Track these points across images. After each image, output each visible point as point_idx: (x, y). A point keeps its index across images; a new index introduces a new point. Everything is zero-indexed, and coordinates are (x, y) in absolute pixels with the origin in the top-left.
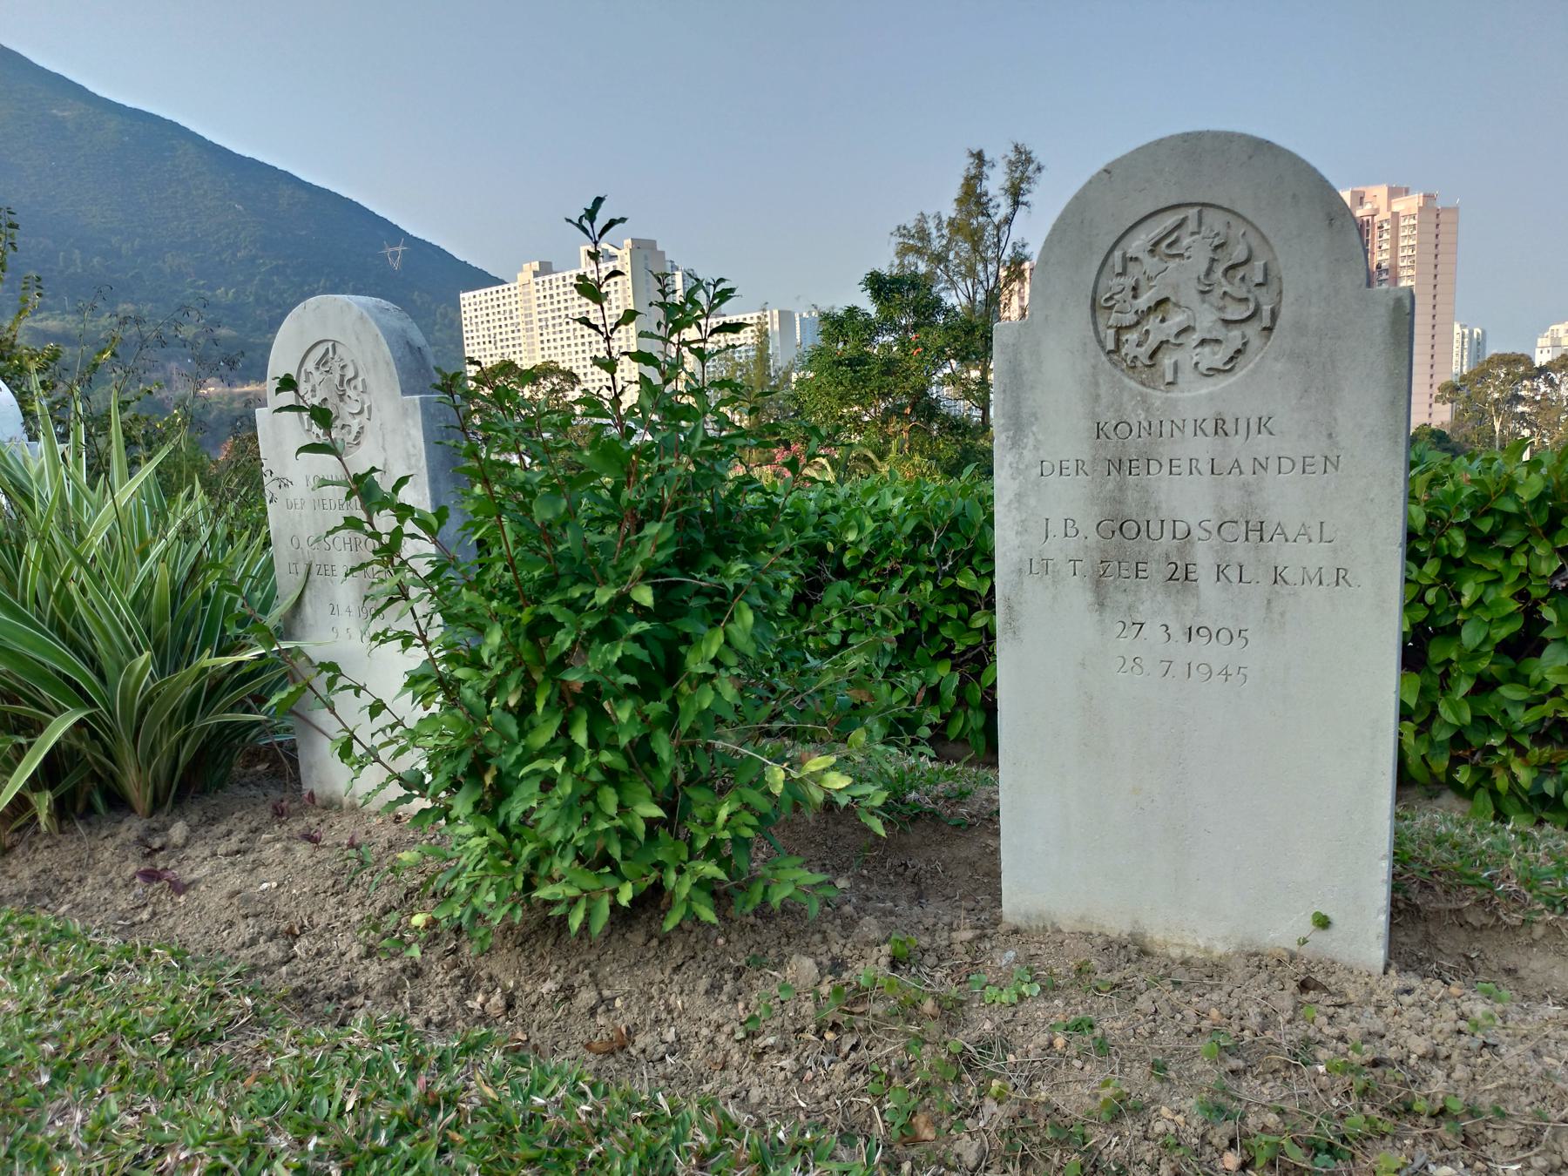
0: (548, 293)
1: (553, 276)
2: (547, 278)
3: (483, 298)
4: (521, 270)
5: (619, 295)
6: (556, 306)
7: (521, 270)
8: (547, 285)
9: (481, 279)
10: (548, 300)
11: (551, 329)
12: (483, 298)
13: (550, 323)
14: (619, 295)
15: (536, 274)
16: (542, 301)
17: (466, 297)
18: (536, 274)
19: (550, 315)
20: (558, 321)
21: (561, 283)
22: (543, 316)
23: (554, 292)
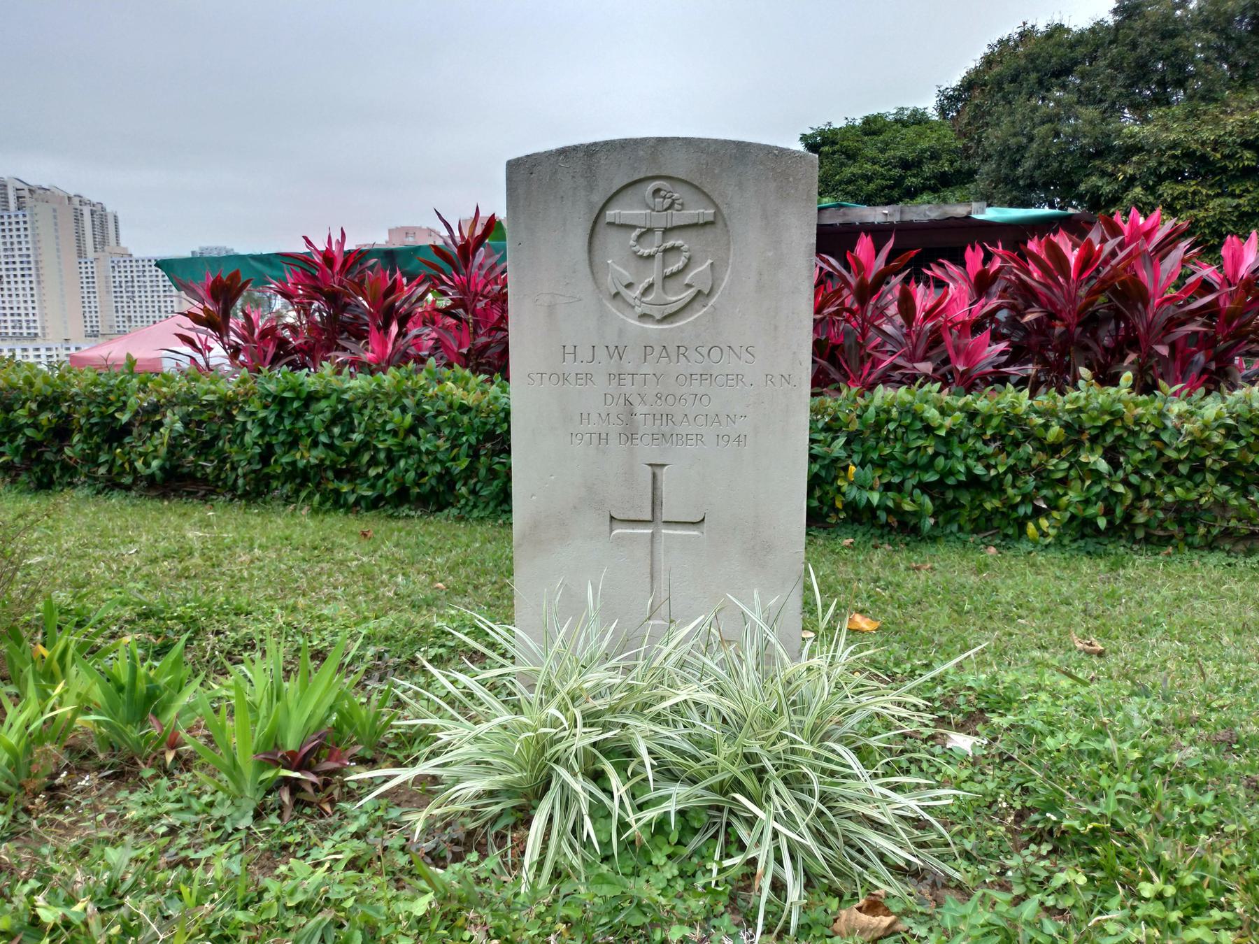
14: (29, 239)
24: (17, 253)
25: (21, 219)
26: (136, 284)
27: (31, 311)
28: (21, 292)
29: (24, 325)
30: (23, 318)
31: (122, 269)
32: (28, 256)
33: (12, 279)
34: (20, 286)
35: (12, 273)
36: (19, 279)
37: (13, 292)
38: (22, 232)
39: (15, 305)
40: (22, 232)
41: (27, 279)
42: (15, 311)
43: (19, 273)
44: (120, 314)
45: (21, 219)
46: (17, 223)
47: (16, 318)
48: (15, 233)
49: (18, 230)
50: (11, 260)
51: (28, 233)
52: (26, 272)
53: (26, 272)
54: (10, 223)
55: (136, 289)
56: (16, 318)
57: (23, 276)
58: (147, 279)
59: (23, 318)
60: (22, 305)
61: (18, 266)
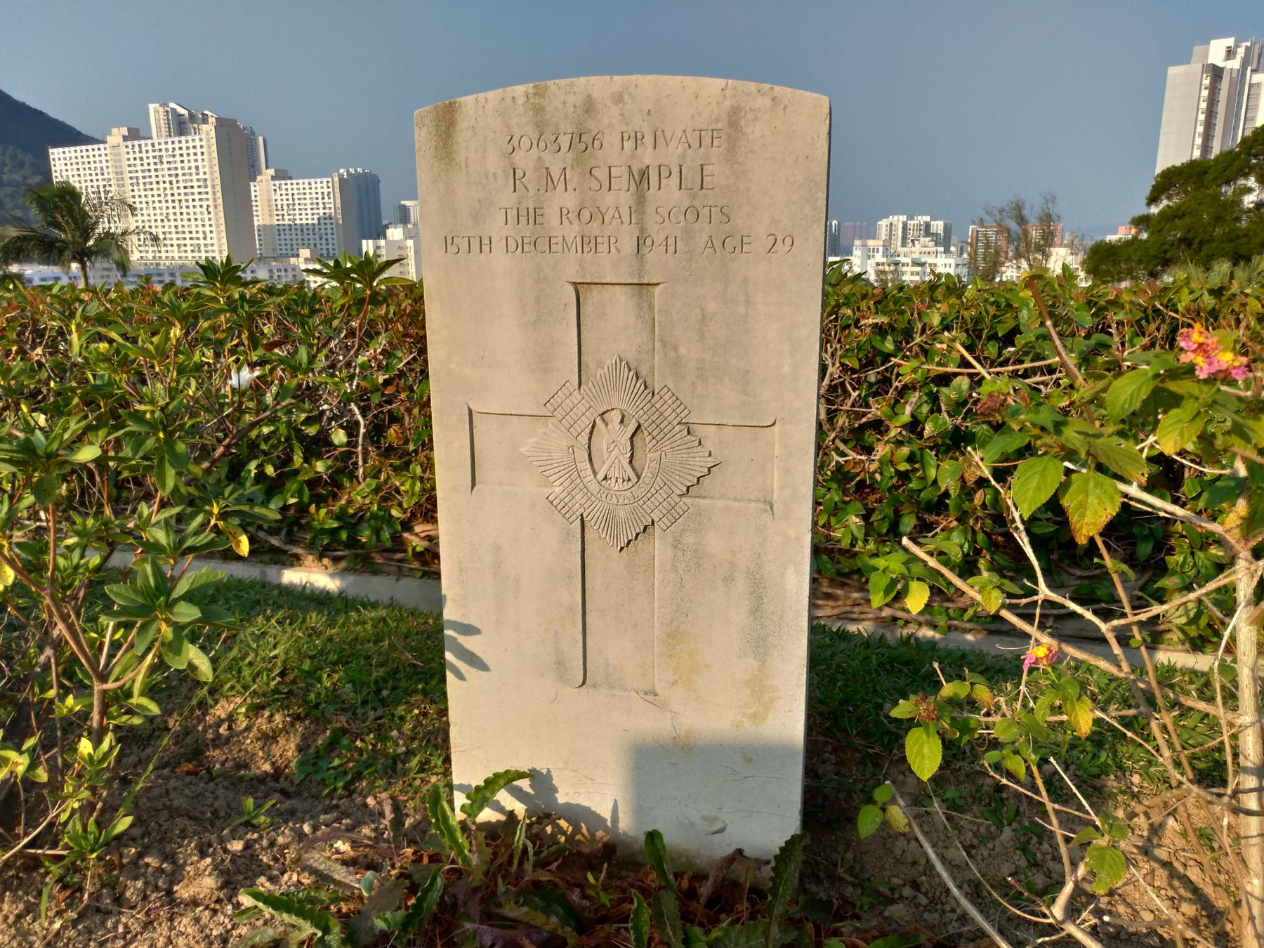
0: (138, 155)
1: (142, 142)
2: (136, 143)
3: (73, 155)
4: (110, 134)
5: (206, 163)
6: (146, 167)
7: (110, 134)
8: (137, 149)
9: (71, 137)
10: (138, 162)
11: (142, 187)
12: (73, 155)
13: (141, 181)
14: (206, 163)
15: (125, 139)
16: (132, 162)
17: (55, 154)
18: (125, 139)
19: (140, 174)
20: (148, 180)
21: (150, 148)
22: (134, 175)
23: (144, 155)
24: (194, 177)
25: (198, 143)
26: (297, 207)
27: (209, 235)
28: (199, 216)
29: (203, 248)
30: (202, 242)
31: (284, 192)
32: (205, 180)
33: (191, 204)
34: (198, 210)
35: (190, 197)
36: (197, 203)
37: (192, 217)
38: (199, 157)
39: (194, 229)
40: (199, 157)
41: (205, 204)
42: (194, 235)
43: (197, 197)
44: (282, 237)
45: (198, 143)
46: (194, 147)
47: (195, 242)
48: (192, 158)
49: (195, 154)
50: (189, 184)
51: (205, 157)
52: (204, 196)
53: (204, 196)
54: (188, 148)
55: (297, 212)
56: (195, 242)
57: (201, 200)
58: (308, 201)
59: (202, 242)
60: (200, 229)
61: (196, 190)
